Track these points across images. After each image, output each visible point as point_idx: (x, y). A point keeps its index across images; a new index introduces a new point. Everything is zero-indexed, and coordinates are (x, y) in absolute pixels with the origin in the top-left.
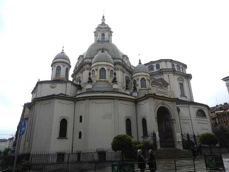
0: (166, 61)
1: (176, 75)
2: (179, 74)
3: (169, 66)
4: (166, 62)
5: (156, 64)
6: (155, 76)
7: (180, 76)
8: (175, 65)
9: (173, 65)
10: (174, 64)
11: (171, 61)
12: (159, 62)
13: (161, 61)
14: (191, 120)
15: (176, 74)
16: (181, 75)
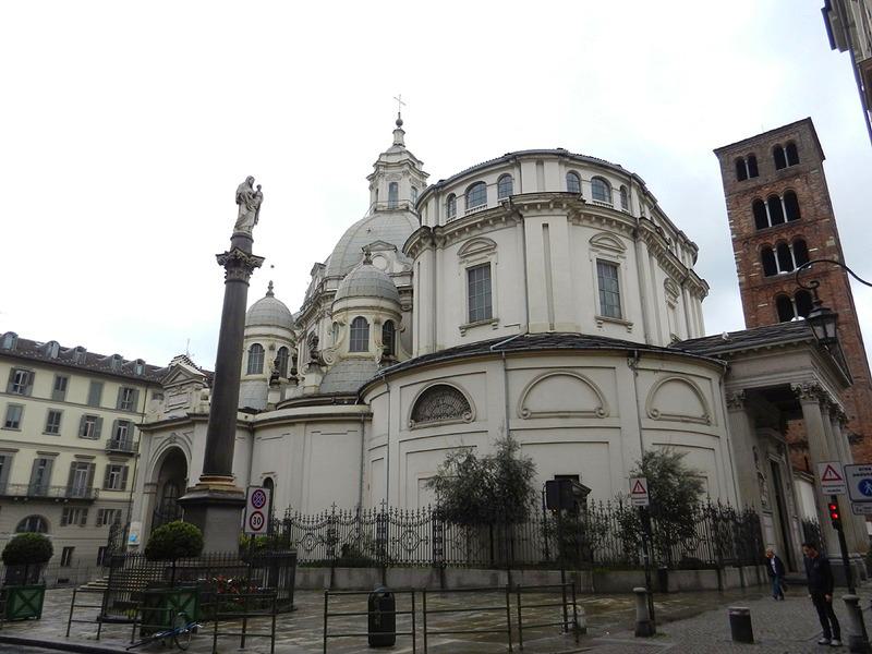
0: (539, 157)
1: (586, 223)
2: (599, 219)
3: (555, 179)
4: (540, 163)
5: (499, 174)
6: (487, 229)
7: (607, 228)
8: (583, 177)
9: (574, 177)
10: (580, 171)
11: (561, 156)
12: (512, 166)
13: (514, 160)
14: (642, 429)
15: (588, 217)
16: (609, 221)
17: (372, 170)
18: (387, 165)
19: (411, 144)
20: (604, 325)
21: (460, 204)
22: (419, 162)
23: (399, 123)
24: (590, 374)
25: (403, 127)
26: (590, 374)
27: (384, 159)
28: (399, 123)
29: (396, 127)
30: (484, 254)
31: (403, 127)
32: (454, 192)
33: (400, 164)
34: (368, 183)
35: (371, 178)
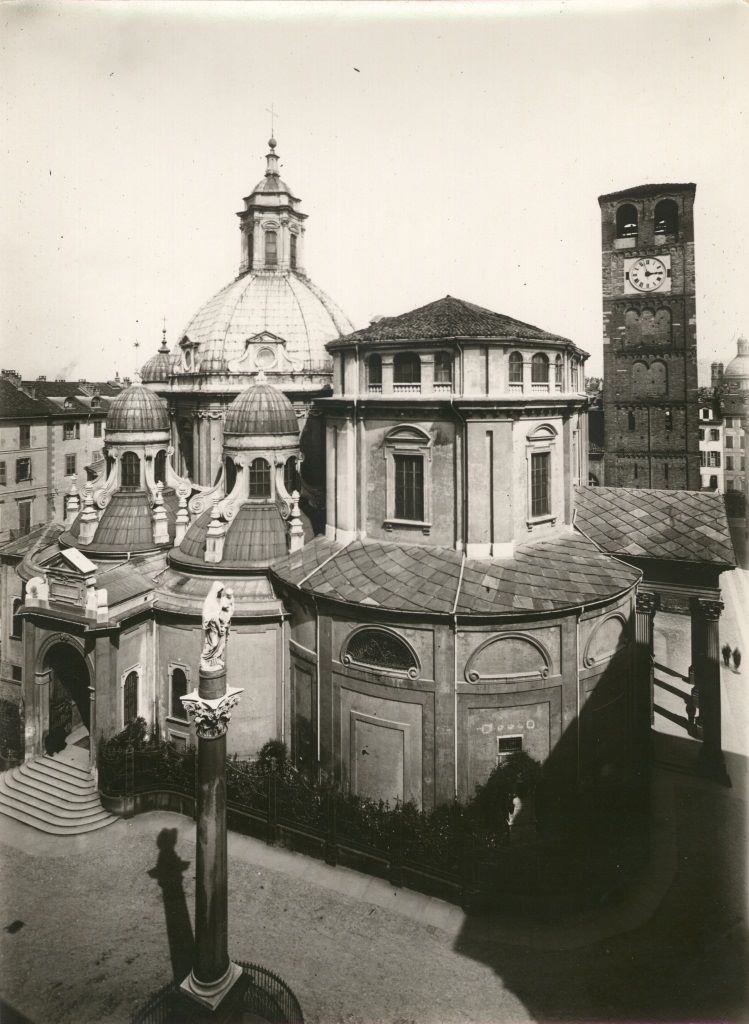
17: (243, 208)
18: (263, 209)
19: (289, 179)
20: (534, 527)
21: (388, 374)
22: (298, 201)
23: (272, 145)
24: (538, 635)
25: (277, 151)
26: (538, 635)
27: (260, 201)
28: (272, 145)
29: (268, 150)
30: (416, 447)
31: (277, 151)
32: (379, 352)
33: (278, 210)
34: (238, 220)
35: (242, 215)
